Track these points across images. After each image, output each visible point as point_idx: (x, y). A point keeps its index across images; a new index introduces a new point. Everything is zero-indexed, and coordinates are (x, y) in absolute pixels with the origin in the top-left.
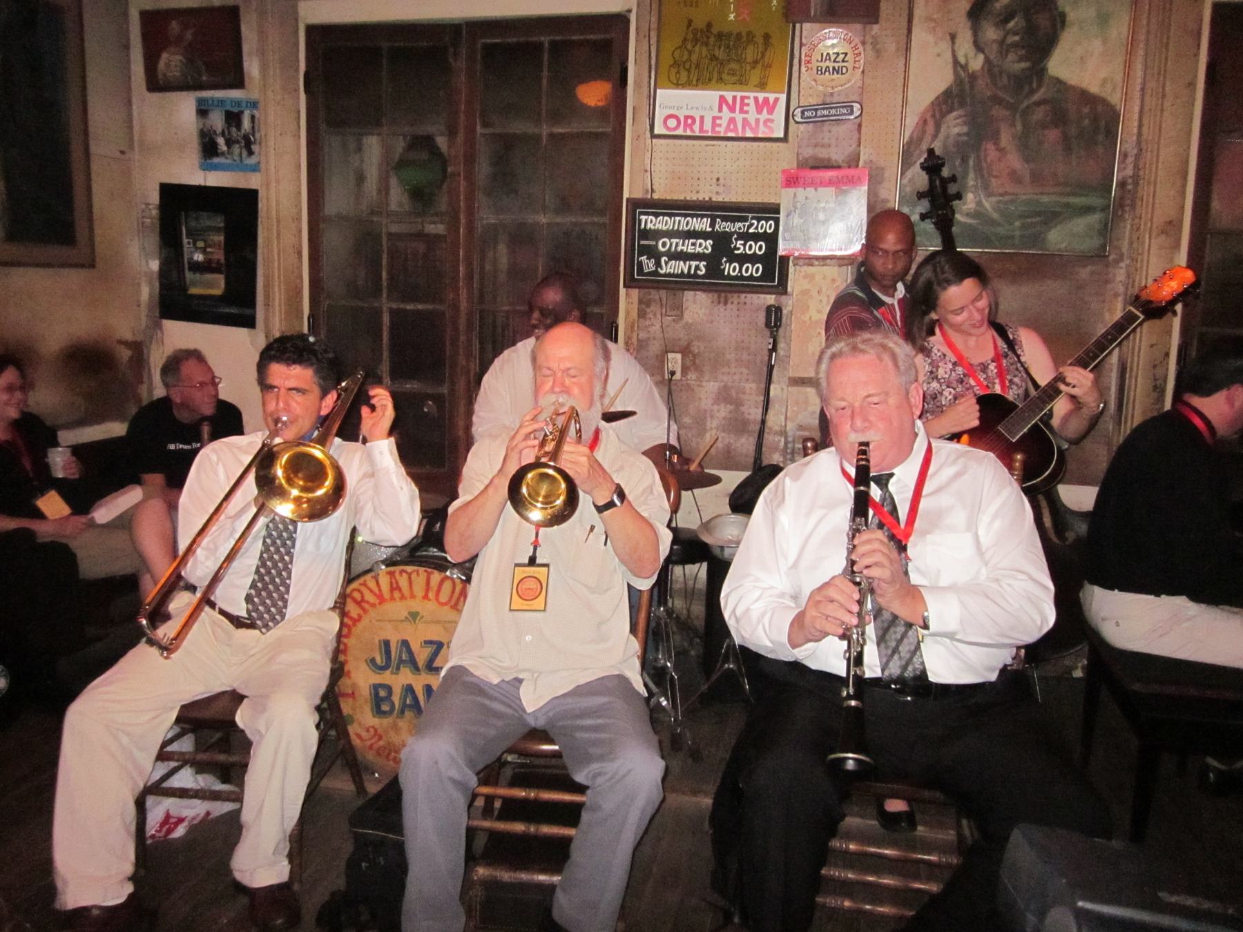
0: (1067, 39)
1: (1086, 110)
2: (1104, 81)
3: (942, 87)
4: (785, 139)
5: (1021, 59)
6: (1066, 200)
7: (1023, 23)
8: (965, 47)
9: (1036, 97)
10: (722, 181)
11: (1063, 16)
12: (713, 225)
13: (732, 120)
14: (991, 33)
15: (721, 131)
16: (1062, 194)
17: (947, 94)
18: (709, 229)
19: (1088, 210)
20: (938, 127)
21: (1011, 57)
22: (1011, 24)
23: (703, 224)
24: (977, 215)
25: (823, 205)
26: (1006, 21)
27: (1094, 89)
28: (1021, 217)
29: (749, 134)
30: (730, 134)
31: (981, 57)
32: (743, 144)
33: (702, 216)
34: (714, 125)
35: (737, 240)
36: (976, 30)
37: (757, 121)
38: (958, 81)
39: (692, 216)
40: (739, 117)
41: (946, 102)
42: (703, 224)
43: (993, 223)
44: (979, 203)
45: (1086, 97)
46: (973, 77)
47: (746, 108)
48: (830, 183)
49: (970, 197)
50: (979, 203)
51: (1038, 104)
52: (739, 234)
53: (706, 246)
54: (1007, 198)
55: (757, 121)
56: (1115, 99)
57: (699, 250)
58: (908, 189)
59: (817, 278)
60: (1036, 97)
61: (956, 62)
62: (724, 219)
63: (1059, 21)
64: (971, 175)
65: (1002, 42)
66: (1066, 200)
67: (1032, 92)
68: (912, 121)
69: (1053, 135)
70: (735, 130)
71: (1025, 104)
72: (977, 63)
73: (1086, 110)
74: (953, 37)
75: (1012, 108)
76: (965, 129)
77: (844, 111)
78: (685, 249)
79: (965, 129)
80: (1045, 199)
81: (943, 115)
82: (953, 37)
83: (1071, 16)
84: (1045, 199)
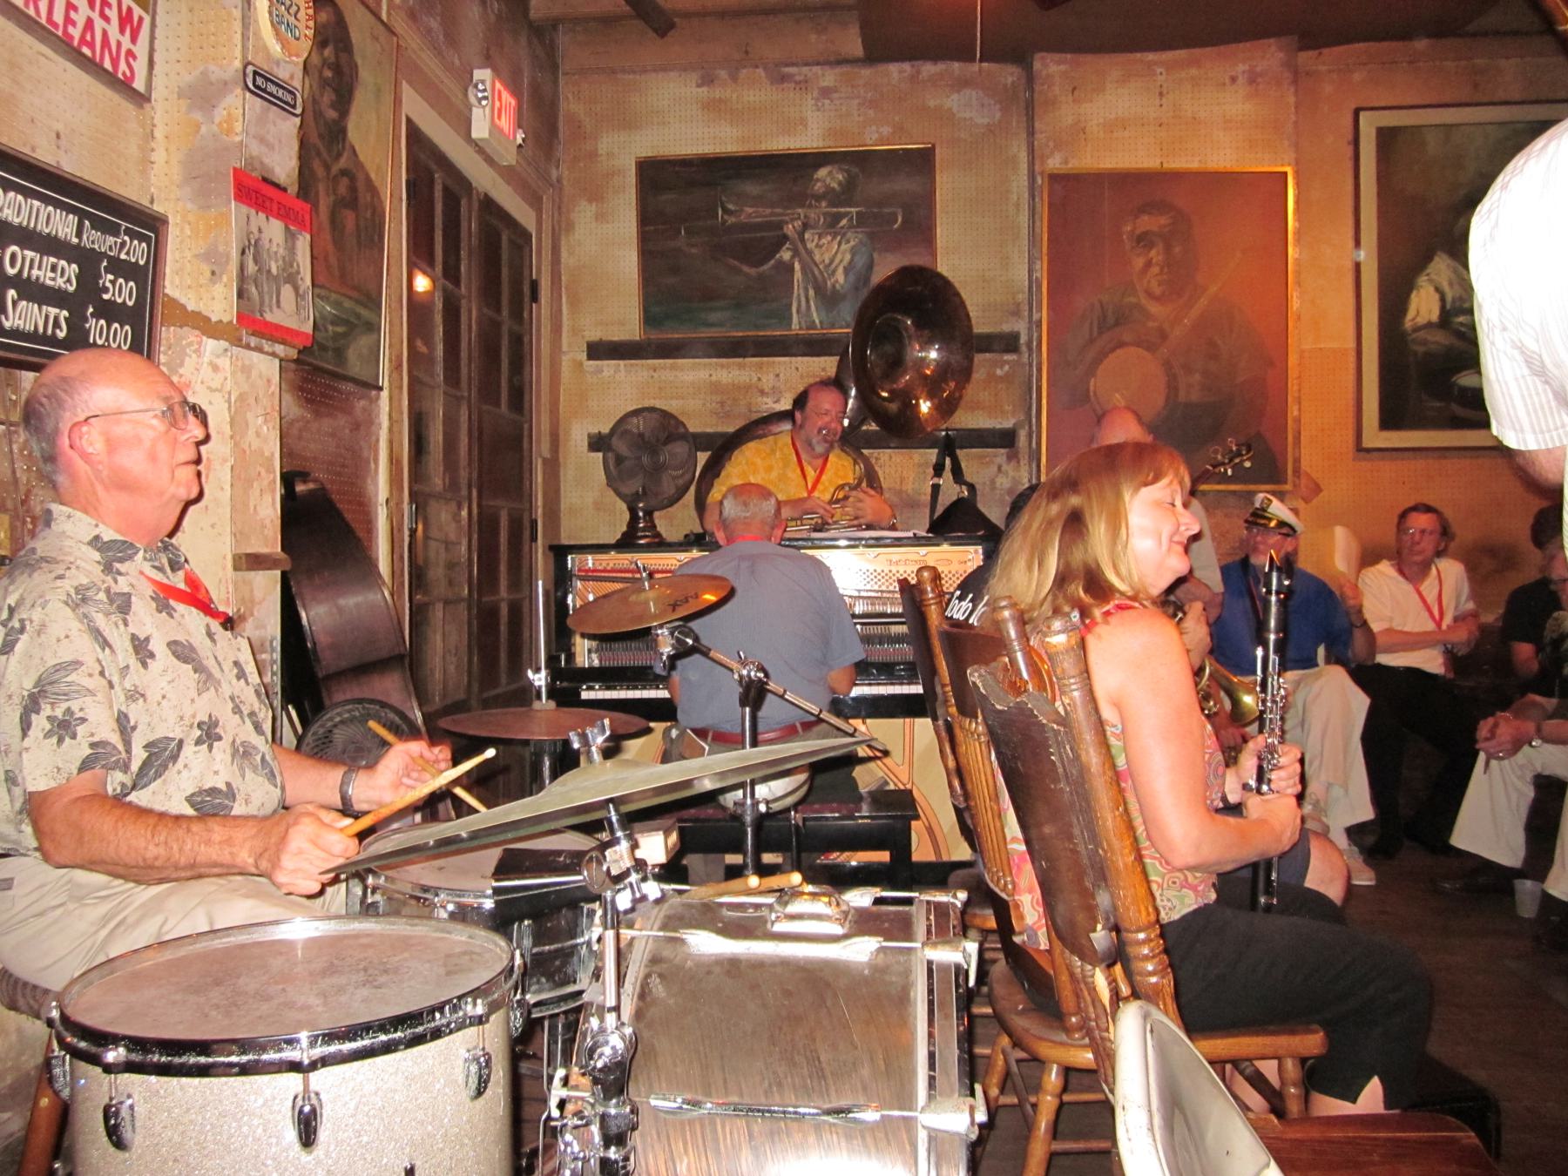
4: (141, 99)
10: (63, 142)
12: (79, 234)
13: (89, 24)
15: (76, 32)
16: (357, 302)
18: (75, 240)
23: (63, 225)
25: (274, 249)
28: (332, 323)
29: (108, 65)
30: (86, 51)
32: (85, 80)
33: (70, 209)
34: (69, 21)
35: (107, 270)
37: (119, 44)
39: (58, 204)
40: (99, 25)
42: (63, 225)
47: (107, 11)
48: (278, 216)
51: (344, 172)
52: (110, 259)
53: (65, 276)
54: (323, 292)
55: (119, 44)
57: (60, 282)
59: (254, 373)
62: (100, 224)
67: (339, 155)
69: (349, 218)
70: (91, 46)
71: (335, 169)
75: (327, 168)
77: (289, 98)
78: (41, 273)
84: (348, 304)
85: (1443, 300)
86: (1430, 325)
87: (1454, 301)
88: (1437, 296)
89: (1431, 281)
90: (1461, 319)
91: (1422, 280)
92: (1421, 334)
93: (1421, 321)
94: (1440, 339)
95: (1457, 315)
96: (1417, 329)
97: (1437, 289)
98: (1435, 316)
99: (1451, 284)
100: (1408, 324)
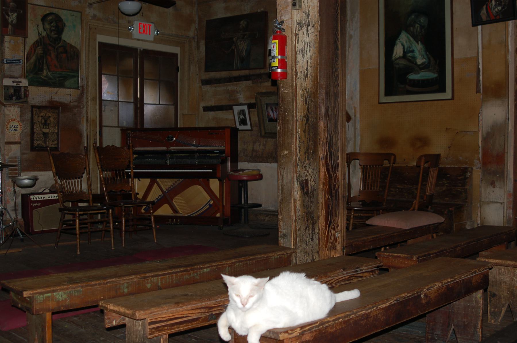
0: (66, 30)
1: (72, 49)
2: (75, 43)
3: (35, 39)
5: (55, 34)
6: (69, 73)
7: (55, 25)
8: (41, 29)
9: (60, 45)
11: (65, 24)
14: (47, 26)
17: (37, 41)
19: (74, 77)
20: (35, 51)
21: (53, 33)
22: (52, 24)
24: (46, 76)
26: (51, 23)
27: (73, 44)
31: (45, 32)
36: (43, 24)
38: (40, 39)
41: (37, 44)
43: (50, 79)
44: (47, 73)
45: (71, 46)
46: (43, 37)
49: (45, 71)
50: (47, 73)
51: (60, 47)
56: (79, 47)
58: (28, 68)
60: (60, 45)
61: (39, 33)
63: (64, 25)
64: (45, 65)
65: (50, 29)
66: (69, 73)
67: (58, 43)
68: (28, 48)
72: (44, 34)
73: (72, 49)
74: (38, 26)
76: (42, 52)
79: (42, 52)
80: (64, 73)
81: (36, 47)
82: (38, 26)
83: (67, 24)
84: (64, 73)
85: (404, 48)
86: (400, 58)
87: (407, 48)
88: (402, 47)
89: (400, 41)
90: (409, 54)
91: (398, 42)
92: (398, 61)
93: (397, 56)
94: (403, 62)
95: (408, 53)
96: (396, 59)
97: (402, 45)
98: (401, 55)
99: (406, 42)
100: (394, 58)
